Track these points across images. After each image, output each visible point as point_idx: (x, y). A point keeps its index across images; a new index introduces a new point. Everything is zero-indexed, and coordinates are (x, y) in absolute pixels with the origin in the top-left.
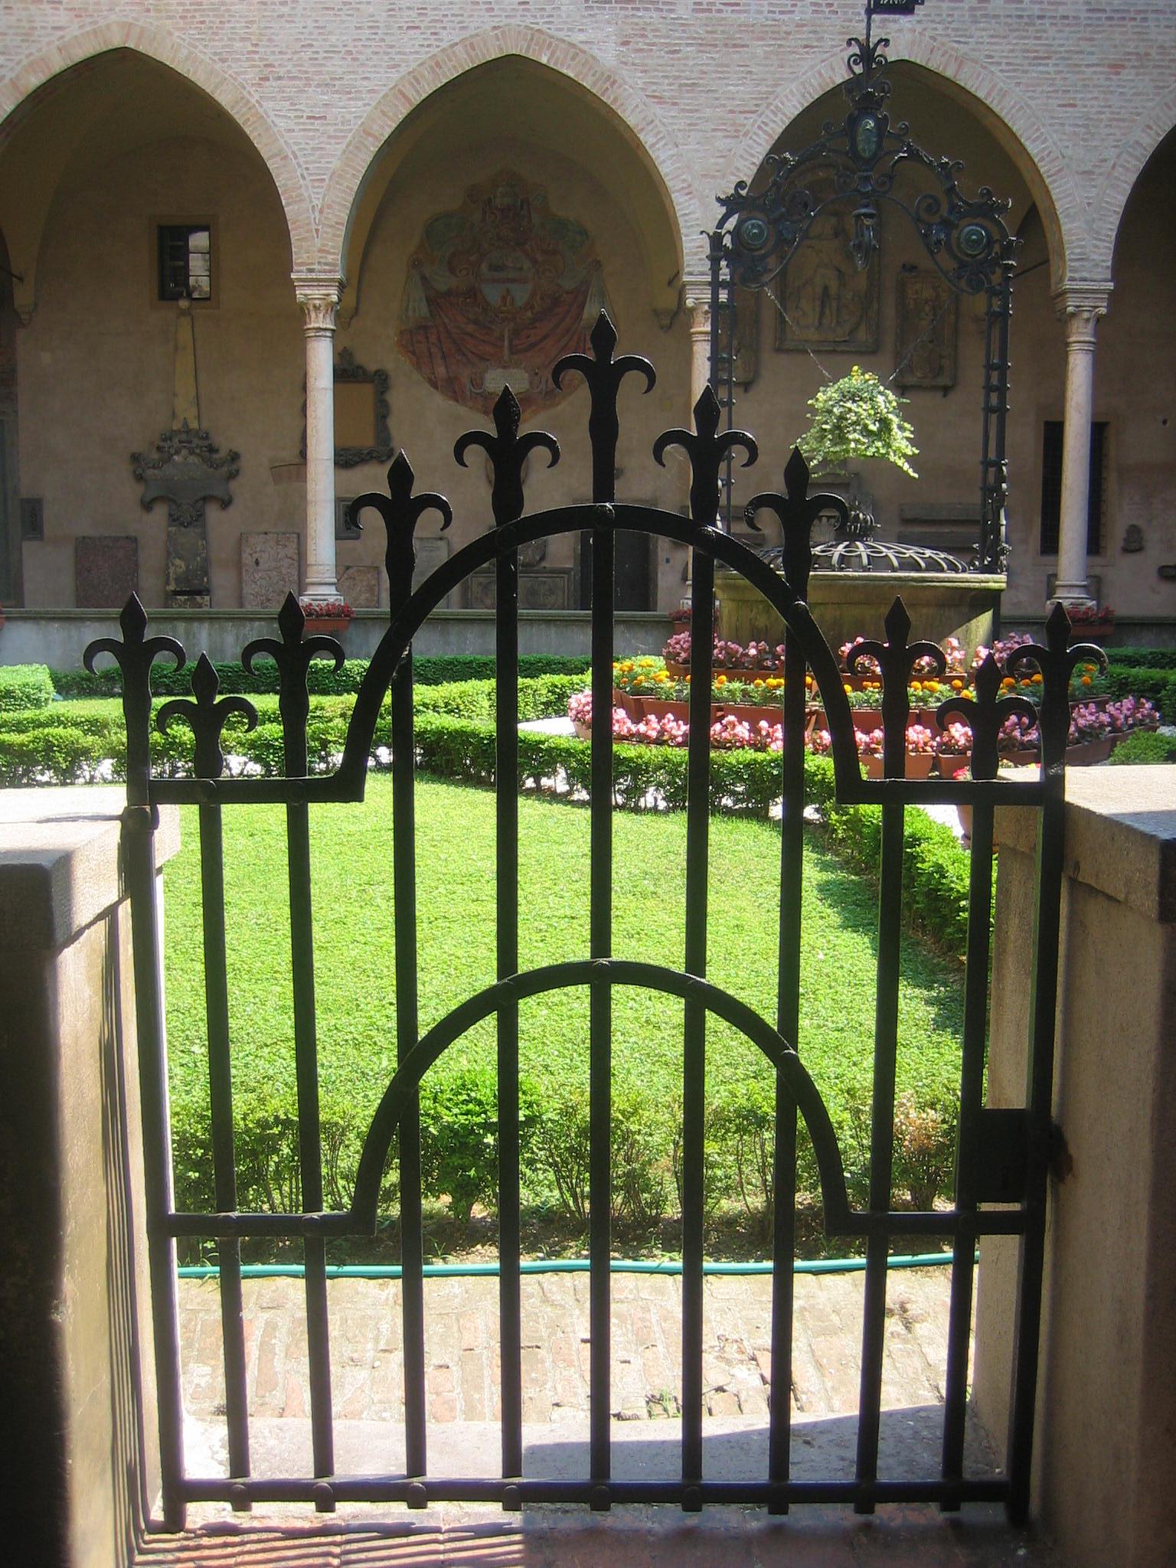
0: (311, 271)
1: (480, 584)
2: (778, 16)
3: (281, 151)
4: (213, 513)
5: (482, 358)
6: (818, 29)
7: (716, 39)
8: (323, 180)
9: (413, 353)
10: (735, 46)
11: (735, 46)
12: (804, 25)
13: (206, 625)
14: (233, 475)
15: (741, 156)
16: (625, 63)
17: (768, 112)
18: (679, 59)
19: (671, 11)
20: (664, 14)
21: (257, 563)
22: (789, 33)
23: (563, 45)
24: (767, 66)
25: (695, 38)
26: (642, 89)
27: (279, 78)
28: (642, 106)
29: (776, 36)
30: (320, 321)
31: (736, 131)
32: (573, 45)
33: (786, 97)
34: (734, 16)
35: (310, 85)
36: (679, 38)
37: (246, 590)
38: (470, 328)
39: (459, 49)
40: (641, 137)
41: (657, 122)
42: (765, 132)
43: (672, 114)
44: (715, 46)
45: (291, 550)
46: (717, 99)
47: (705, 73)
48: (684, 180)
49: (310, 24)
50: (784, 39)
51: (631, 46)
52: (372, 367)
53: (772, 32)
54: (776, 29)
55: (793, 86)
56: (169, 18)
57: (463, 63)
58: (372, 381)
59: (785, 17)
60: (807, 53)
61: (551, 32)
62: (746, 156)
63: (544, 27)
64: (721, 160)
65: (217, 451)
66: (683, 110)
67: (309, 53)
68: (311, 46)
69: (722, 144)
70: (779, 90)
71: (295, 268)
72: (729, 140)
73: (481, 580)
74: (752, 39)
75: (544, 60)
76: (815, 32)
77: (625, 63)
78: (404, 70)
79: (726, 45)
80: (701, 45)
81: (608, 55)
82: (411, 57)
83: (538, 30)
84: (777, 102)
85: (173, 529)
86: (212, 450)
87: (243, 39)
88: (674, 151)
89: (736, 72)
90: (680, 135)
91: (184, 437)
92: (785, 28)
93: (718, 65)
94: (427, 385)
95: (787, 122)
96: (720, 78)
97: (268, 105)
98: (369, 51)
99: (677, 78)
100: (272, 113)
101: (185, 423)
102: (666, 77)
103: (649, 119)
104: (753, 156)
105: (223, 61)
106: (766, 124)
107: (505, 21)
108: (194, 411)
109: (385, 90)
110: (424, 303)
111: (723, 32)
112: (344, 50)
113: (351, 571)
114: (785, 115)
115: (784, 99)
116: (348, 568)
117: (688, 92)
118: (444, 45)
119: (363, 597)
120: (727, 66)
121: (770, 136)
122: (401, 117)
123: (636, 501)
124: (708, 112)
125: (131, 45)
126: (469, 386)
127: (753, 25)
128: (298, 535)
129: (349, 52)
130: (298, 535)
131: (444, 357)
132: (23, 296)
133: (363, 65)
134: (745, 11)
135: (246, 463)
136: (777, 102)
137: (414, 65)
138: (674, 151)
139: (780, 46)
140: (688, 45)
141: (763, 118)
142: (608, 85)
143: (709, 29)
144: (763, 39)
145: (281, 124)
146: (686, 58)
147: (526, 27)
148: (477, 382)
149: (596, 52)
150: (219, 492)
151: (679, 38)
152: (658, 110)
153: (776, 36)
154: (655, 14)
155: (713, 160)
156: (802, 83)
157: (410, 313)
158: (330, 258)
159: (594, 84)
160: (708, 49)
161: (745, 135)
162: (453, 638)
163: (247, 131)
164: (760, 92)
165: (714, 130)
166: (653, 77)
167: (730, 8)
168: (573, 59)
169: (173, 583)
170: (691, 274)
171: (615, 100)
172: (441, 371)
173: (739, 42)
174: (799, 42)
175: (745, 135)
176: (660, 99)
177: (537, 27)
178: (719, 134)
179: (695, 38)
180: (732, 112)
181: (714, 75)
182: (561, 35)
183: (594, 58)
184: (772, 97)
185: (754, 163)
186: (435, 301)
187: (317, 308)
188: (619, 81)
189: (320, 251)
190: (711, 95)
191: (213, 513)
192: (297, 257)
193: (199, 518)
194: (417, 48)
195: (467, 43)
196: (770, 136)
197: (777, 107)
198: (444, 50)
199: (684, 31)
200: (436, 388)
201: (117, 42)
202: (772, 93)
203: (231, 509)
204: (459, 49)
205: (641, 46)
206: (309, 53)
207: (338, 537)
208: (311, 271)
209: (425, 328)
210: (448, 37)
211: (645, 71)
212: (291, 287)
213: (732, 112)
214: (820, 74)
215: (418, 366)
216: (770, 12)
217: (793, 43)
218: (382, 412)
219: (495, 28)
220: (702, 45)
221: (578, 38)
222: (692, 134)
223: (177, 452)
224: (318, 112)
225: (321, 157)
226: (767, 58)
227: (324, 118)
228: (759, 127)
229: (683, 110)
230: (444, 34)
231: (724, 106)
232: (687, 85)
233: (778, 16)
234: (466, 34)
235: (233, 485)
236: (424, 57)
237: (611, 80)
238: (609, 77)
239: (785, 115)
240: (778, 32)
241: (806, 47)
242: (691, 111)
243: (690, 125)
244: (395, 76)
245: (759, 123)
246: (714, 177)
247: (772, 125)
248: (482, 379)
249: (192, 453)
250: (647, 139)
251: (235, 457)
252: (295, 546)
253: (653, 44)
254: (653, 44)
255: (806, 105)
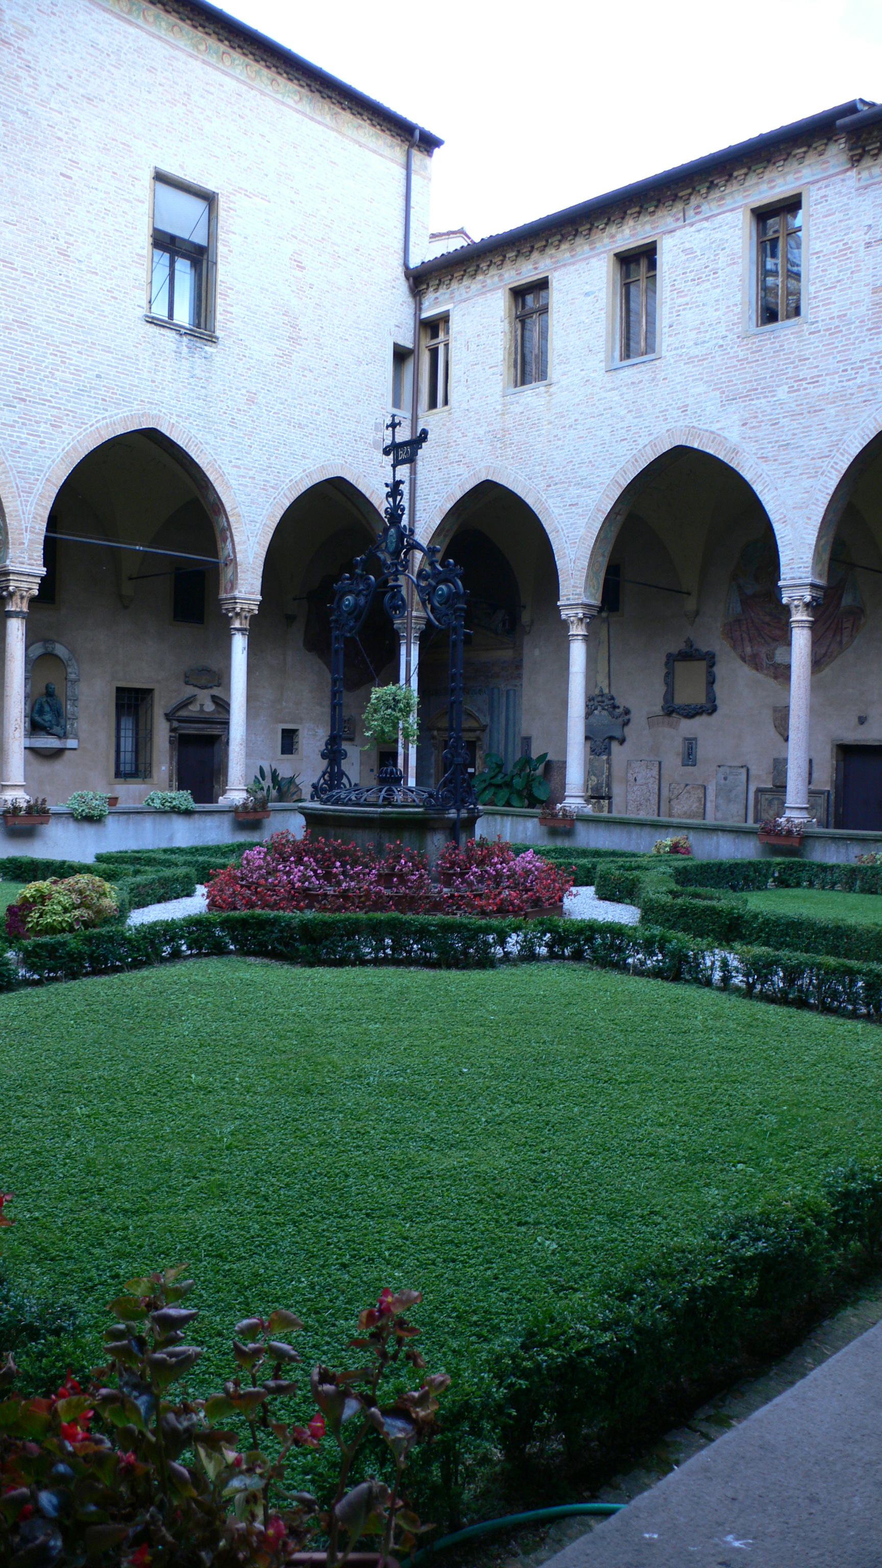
0: (568, 599)
1: (767, 799)
2: (845, 384)
3: (556, 528)
4: (615, 746)
5: (775, 639)
6: (874, 386)
7: (802, 409)
8: (575, 543)
9: (732, 638)
10: (815, 411)
11: (815, 411)
12: (864, 386)
13: (510, 818)
14: (626, 723)
15: (820, 490)
16: (744, 438)
17: (838, 455)
18: (778, 428)
19: (774, 396)
20: (769, 399)
21: (635, 780)
22: (852, 394)
23: (707, 434)
24: (836, 421)
25: (788, 412)
26: (755, 454)
27: (556, 484)
28: (754, 466)
29: (844, 398)
30: (577, 630)
31: (816, 472)
32: (712, 432)
33: (851, 441)
34: (815, 390)
35: (570, 486)
36: (779, 414)
37: (629, 797)
38: (767, 619)
39: (648, 447)
40: (754, 487)
41: (764, 475)
42: (836, 470)
43: (774, 467)
44: (802, 414)
45: (655, 772)
46: (803, 451)
47: (795, 434)
48: (782, 513)
49: (572, 448)
50: (850, 399)
51: (748, 426)
52: (705, 649)
53: (841, 396)
54: (843, 393)
55: (856, 432)
56: (507, 459)
57: (651, 456)
58: (704, 659)
59: (850, 383)
60: (866, 406)
61: (700, 427)
62: (823, 489)
63: (695, 424)
64: (806, 495)
65: (618, 707)
66: (780, 464)
67: (570, 467)
68: (571, 462)
69: (806, 483)
70: (845, 437)
71: (782, 577)
72: (810, 480)
73: (767, 796)
74: (827, 404)
75: (695, 446)
76: (871, 389)
77: (744, 438)
78: (618, 467)
79: (809, 412)
80: (793, 415)
81: (733, 435)
82: (622, 458)
83: (693, 427)
84: (845, 446)
85: (592, 757)
86: (615, 707)
87: (539, 465)
88: (775, 493)
89: (816, 430)
90: (779, 481)
91: (600, 699)
92: (850, 391)
93: (804, 427)
94: (739, 662)
95: (852, 460)
96: (805, 436)
97: (550, 501)
98: (600, 459)
99: (777, 442)
100: (552, 506)
101: (601, 690)
102: (769, 443)
103: (759, 474)
104: (827, 488)
105: (530, 479)
106: (836, 463)
107: (674, 425)
108: (606, 682)
109: (608, 482)
110: (739, 604)
111: (807, 403)
112: (587, 461)
113: (688, 787)
114: (850, 454)
115: (849, 443)
116: (687, 785)
117: (784, 450)
118: (640, 447)
119: (695, 805)
120: (810, 426)
121: (839, 471)
122: (616, 497)
123: (875, 740)
124: (797, 462)
125: (489, 478)
126: (765, 658)
127: (828, 394)
128: (660, 763)
129: (590, 462)
130: (660, 763)
131: (750, 641)
132: (525, 617)
133: (598, 468)
134: (823, 385)
135: (634, 716)
136: (845, 446)
137: (624, 463)
138: (775, 493)
139: (847, 405)
140: (784, 417)
141: (835, 459)
142: (734, 455)
143: (799, 403)
144: (834, 402)
145: (556, 511)
146: (783, 427)
147: (686, 426)
148: (770, 656)
149: (726, 434)
150: (617, 734)
151: (779, 414)
152: (764, 466)
153: (844, 398)
154: (763, 401)
155: (800, 496)
156: (862, 429)
157: (731, 611)
158: (578, 591)
159: (725, 456)
160: (797, 417)
161: (822, 474)
162: (634, 836)
163: (540, 518)
164: (832, 441)
165: (801, 474)
166: (763, 444)
167: (812, 386)
168: (713, 442)
169: (590, 791)
170: (785, 579)
171: (738, 464)
172: (748, 650)
173: (818, 408)
174: (860, 399)
175: (822, 474)
176: (764, 458)
177: (691, 425)
178: (805, 476)
179: (788, 412)
180: (813, 459)
181: (802, 435)
182: (705, 427)
183: (725, 438)
184: (841, 443)
185: (828, 494)
186: (746, 602)
187: (572, 622)
188: (741, 451)
189: (574, 587)
190: (799, 450)
191: (615, 746)
192: (561, 593)
193: (607, 750)
194: (625, 452)
195: (713, 436)
196: (839, 471)
197: (844, 450)
198: (640, 450)
199: (782, 408)
200: (745, 662)
201: (483, 478)
202: (840, 440)
203: (626, 744)
204: (648, 447)
205: (754, 424)
206: (570, 467)
207: (785, 760)
208: (568, 599)
209: (739, 621)
210: (642, 442)
211: (756, 441)
212: (557, 610)
213: (813, 459)
214: (876, 420)
215: (734, 647)
216: (840, 382)
217: (856, 401)
218: (711, 681)
219: (668, 431)
220: (794, 415)
221: (715, 427)
222: (787, 479)
223: (596, 709)
224: (574, 501)
225: (575, 528)
226: (836, 416)
227: (577, 504)
228: (832, 467)
229: (780, 464)
230: (640, 441)
231: (808, 455)
232: (782, 446)
233: (845, 384)
234: (652, 438)
235: (626, 729)
236: (629, 457)
237: (735, 451)
238: (734, 449)
239: (850, 454)
240: (845, 395)
241: (865, 401)
242: (786, 463)
243: (786, 473)
244: (614, 472)
245: (832, 464)
246: (801, 508)
247: (840, 463)
248: (774, 654)
249: (603, 709)
250: (757, 488)
251: (627, 712)
252: (657, 769)
253: (762, 421)
254: (762, 421)
255: (865, 444)
